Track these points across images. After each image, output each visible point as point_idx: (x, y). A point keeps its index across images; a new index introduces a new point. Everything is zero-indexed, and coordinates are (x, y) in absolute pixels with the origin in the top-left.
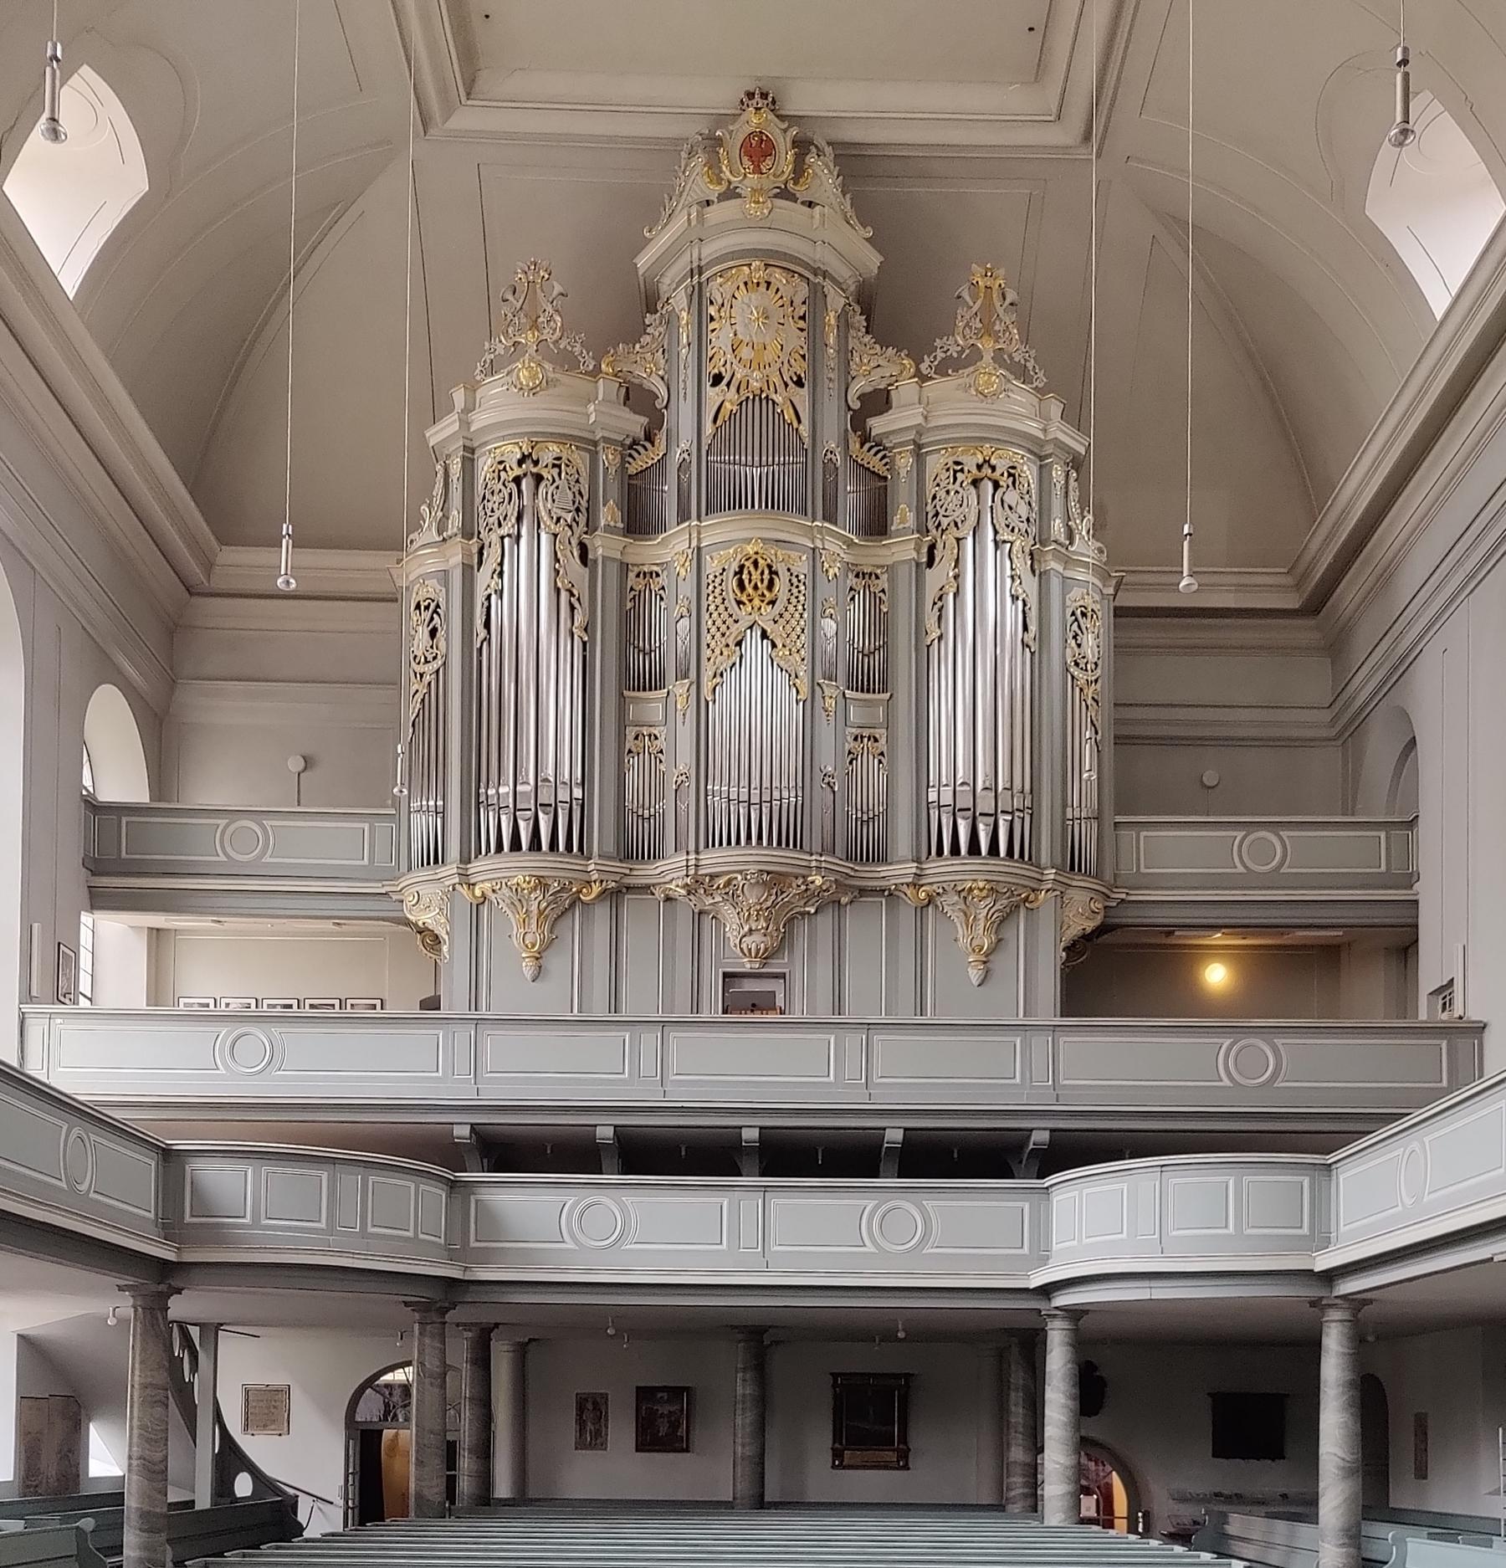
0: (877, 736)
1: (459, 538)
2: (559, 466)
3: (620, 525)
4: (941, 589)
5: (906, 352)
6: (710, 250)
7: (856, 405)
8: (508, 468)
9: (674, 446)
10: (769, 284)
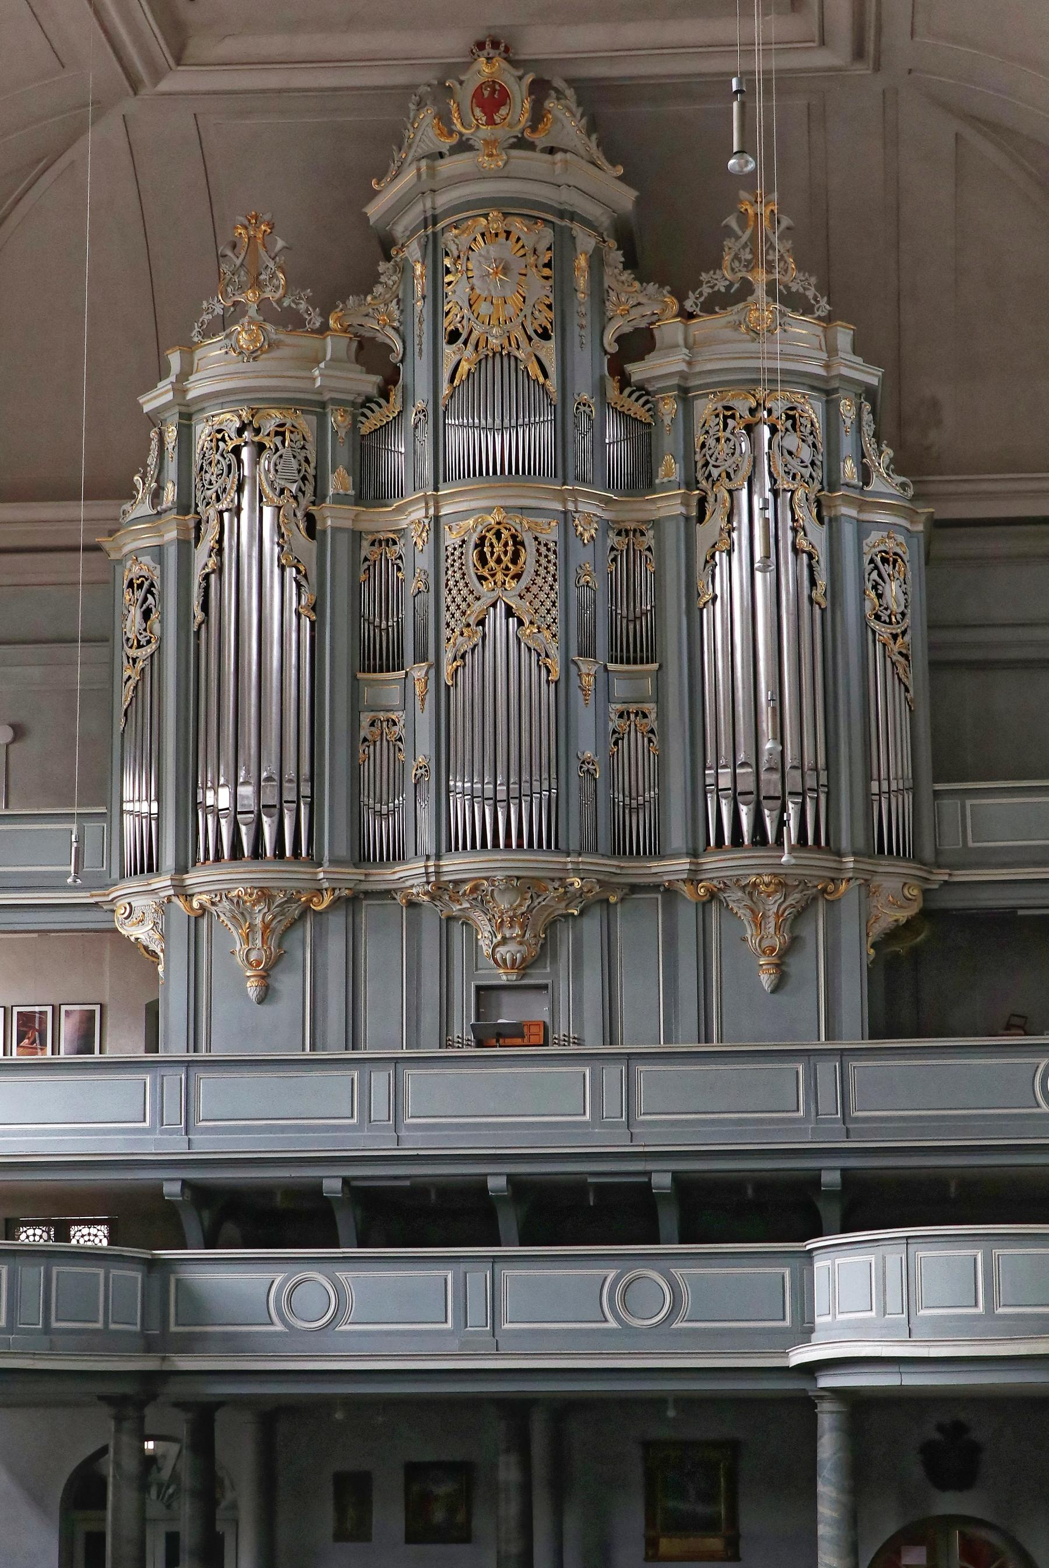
0: (647, 712)
1: (172, 515)
2: (282, 434)
3: (351, 492)
4: (713, 546)
5: (668, 288)
6: (445, 199)
7: (613, 348)
8: (227, 438)
9: (410, 407)
10: (508, 233)
